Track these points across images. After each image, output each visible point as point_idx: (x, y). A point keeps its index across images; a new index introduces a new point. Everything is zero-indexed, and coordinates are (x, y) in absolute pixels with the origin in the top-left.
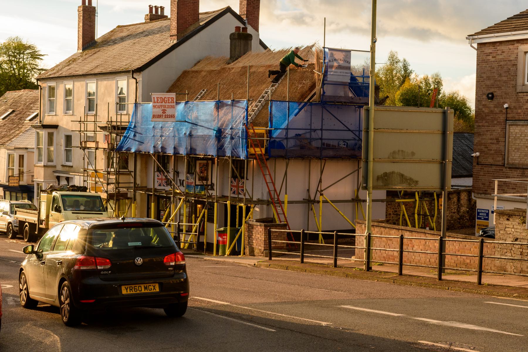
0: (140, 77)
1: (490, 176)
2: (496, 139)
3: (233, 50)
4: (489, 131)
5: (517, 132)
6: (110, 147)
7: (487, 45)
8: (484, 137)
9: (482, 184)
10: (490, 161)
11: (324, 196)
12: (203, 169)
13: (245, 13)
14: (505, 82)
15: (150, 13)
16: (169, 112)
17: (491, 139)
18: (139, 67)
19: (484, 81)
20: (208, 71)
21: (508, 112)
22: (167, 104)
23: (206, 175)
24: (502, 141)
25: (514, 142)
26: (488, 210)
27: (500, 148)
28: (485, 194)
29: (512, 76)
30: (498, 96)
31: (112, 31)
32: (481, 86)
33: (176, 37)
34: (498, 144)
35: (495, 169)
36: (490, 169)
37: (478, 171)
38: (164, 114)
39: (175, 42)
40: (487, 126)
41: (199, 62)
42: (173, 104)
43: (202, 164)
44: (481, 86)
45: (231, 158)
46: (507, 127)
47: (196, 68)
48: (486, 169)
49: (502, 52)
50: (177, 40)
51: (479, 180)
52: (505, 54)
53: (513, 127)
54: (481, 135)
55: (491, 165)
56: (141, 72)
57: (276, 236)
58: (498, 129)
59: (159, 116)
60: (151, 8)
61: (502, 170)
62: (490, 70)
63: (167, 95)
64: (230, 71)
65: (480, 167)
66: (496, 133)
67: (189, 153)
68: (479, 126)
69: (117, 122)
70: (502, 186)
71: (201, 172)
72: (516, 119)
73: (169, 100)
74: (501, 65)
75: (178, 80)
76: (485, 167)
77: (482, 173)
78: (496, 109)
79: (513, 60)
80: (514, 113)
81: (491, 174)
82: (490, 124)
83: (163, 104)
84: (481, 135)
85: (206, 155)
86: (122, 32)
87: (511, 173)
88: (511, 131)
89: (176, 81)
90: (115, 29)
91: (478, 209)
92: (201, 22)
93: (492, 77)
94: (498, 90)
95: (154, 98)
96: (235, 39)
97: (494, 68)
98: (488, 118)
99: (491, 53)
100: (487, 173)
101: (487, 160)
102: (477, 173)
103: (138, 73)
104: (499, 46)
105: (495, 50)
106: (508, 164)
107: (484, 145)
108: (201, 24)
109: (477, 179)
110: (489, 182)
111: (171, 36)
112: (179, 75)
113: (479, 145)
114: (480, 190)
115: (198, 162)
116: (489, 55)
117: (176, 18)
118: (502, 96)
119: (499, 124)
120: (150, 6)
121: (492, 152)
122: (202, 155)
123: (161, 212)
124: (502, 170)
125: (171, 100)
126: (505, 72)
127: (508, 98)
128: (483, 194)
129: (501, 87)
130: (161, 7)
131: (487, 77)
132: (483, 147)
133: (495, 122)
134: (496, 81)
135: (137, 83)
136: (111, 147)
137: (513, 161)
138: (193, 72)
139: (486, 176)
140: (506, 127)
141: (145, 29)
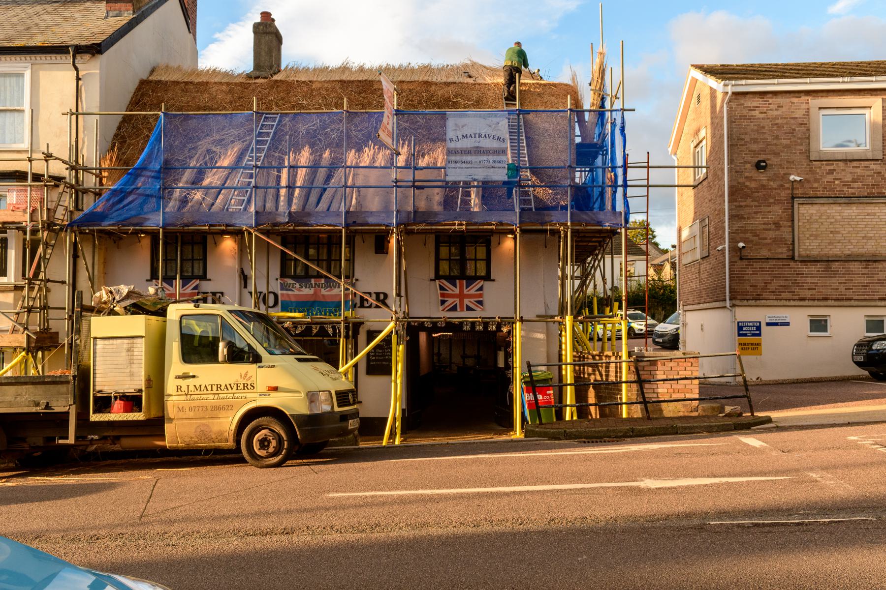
0: (92, 68)
1: (767, 274)
2: (774, 224)
3: (263, 54)
4: (761, 212)
5: (812, 214)
7: (748, 96)
8: (751, 221)
9: (751, 286)
10: (765, 253)
14: (788, 147)
17: (764, 224)
18: (89, 44)
19: (746, 145)
21: (795, 186)
24: (785, 226)
25: (808, 227)
26: (760, 322)
27: (782, 235)
28: (756, 300)
29: (799, 138)
30: (775, 165)
32: (741, 151)
34: (779, 230)
35: (774, 265)
36: (764, 265)
37: (742, 268)
40: (756, 206)
44: (741, 151)
46: (796, 206)
48: (757, 265)
49: (778, 107)
50: (134, 12)
51: (746, 280)
52: (784, 109)
53: (805, 206)
54: (745, 218)
55: (768, 259)
58: (777, 211)
61: (789, 265)
62: (758, 131)
65: (745, 262)
66: (773, 215)
68: (741, 206)
70: (790, 286)
72: (811, 195)
74: (776, 124)
76: (756, 262)
77: (749, 271)
78: (771, 183)
79: (800, 118)
80: (805, 188)
81: (768, 271)
82: (762, 203)
84: (745, 218)
87: (806, 268)
88: (801, 212)
91: (738, 323)
93: (761, 139)
94: (774, 157)
97: (764, 127)
98: (756, 194)
99: (757, 107)
100: (759, 271)
101: (759, 253)
102: (739, 271)
103: (87, 57)
104: (772, 98)
105: (766, 104)
106: (799, 256)
107: (750, 233)
109: (739, 280)
110: (765, 283)
113: (741, 233)
114: (746, 295)
116: (755, 110)
118: (781, 165)
119: (778, 204)
121: (769, 241)
124: (789, 265)
126: (786, 133)
127: (792, 168)
128: (752, 300)
129: (779, 153)
131: (751, 139)
132: (749, 235)
133: (772, 200)
134: (768, 145)
135: (78, 79)
137: (809, 252)
139: (757, 274)
140: (793, 206)
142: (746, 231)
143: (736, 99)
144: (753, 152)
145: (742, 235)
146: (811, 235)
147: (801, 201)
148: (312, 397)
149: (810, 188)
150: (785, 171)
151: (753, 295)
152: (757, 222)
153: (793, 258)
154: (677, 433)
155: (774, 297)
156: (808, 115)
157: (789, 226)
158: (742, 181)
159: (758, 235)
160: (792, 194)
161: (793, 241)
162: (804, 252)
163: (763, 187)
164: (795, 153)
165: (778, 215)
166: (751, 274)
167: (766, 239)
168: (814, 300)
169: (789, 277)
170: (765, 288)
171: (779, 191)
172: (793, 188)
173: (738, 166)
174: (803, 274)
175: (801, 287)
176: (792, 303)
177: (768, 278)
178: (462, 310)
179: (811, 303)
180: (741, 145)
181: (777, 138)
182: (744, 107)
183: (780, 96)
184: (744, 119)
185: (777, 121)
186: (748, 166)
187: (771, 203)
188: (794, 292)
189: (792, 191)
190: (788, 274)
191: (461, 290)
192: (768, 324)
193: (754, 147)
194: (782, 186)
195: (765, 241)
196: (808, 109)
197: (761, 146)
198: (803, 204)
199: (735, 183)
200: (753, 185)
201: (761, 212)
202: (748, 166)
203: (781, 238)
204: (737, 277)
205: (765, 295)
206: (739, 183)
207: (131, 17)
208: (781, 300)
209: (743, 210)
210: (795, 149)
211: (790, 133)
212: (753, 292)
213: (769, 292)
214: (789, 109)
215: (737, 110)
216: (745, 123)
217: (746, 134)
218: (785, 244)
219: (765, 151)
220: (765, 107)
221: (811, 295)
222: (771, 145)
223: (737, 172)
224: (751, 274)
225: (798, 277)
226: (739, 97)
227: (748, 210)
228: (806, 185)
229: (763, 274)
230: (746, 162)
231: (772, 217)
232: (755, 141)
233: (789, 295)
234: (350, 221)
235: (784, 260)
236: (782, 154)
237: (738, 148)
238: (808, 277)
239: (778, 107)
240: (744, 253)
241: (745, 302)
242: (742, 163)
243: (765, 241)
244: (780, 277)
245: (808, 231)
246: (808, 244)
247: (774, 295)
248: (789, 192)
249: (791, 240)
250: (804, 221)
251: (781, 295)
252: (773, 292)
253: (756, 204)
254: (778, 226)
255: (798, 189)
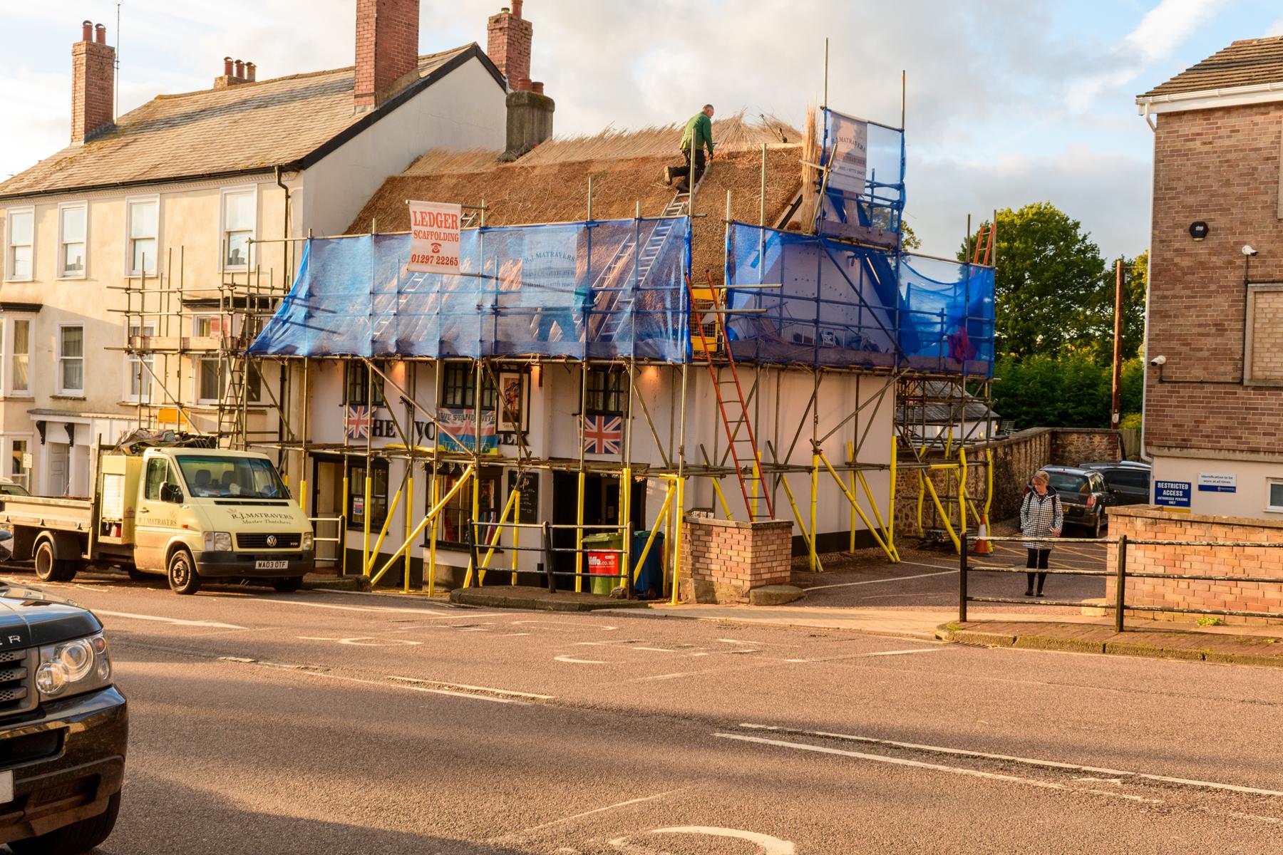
0: (296, 183)
1: (1199, 407)
2: (1215, 325)
3: (515, 131)
4: (1196, 306)
5: (1277, 309)
6: (229, 346)
7: (1185, 117)
8: (1181, 321)
9: (1174, 426)
10: (1198, 373)
11: (823, 455)
12: (512, 393)
13: (504, 62)
14: (1242, 198)
15: (226, 73)
16: (447, 249)
17: (1200, 325)
18: (299, 158)
19: (1179, 198)
20: (460, 176)
21: (1251, 264)
22: (443, 230)
23: (517, 408)
24: (1232, 330)
25: (1269, 330)
26: (1189, 484)
27: (1227, 344)
28: (1182, 448)
29: (1262, 183)
30: (1222, 229)
31: (147, 106)
32: (1169, 208)
33: (373, 98)
34: (1222, 335)
35: (1211, 392)
36: (1198, 392)
37: (1161, 396)
38: (435, 255)
39: (370, 109)
40: (1188, 297)
41: (417, 160)
42: (454, 231)
43: (510, 382)
44: (1169, 208)
45: (633, 362)
46: (1250, 296)
47: (416, 172)
48: (1185, 392)
49: (1232, 131)
50: (376, 105)
51: (1166, 416)
52: (1239, 136)
53: (1266, 296)
54: (1170, 316)
55: (1202, 382)
56: (302, 171)
57: (772, 553)
58: (1221, 305)
59: (425, 260)
60: (229, 65)
61: (1235, 393)
62: (1197, 173)
63: (442, 207)
64: (528, 172)
65: (1168, 387)
66: (1214, 311)
67: (489, 352)
68: (1165, 297)
69: (249, 286)
70: (1236, 428)
71: (509, 401)
72: (1276, 278)
73: (446, 221)
74: (1227, 161)
75: (380, 195)
76: (1184, 387)
77: (1173, 402)
78: (1214, 259)
79: (1266, 148)
80: (1267, 266)
81: (1202, 402)
82: (1197, 292)
83: (435, 229)
84: (1170, 316)
85: (548, 357)
86: (179, 105)
87: (1262, 399)
88: (1259, 305)
89: (374, 198)
90: (152, 102)
91: (1157, 482)
92: (422, 70)
93: (1202, 187)
94: (1221, 215)
95: (415, 212)
96: (519, 106)
97: (1207, 167)
98: (1189, 278)
99: (1198, 134)
100: (1188, 402)
101: (1190, 373)
102: (1158, 401)
103: (293, 174)
104: (1222, 118)
105: (1212, 128)
106: (1251, 379)
107: (1179, 340)
108: (423, 74)
109: (1157, 415)
110: (1196, 422)
111: (356, 97)
112: (380, 187)
113: (1164, 339)
114: (1167, 439)
115: (503, 376)
116: (1194, 140)
117: (373, 54)
118: (1231, 229)
119: (1223, 292)
120: (226, 59)
121: (1205, 354)
122: (534, 357)
123: (356, 499)
124: (1235, 393)
125: (450, 221)
126: (1242, 175)
127: (1248, 233)
128: (1176, 447)
129: (1229, 210)
130: (249, 64)
131: (1187, 188)
132: (1175, 344)
133: (1213, 287)
134: (1212, 196)
135: (288, 197)
136: (232, 345)
137: (1268, 373)
138: (416, 178)
139: (1185, 407)
140: (1246, 296)
141: (244, 97)
142: (1170, 337)
143: (1167, 123)
144: (1189, 209)
145: (1164, 344)
146: (1274, 345)
147: (1258, 287)
148: (209, 535)
149: (1276, 266)
150: (1238, 238)
151: (1177, 440)
152: (1188, 322)
153: (1241, 383)
154: (535, 608)
155: (1210, 445)
156: (1279, 143)
157: (1239, 330)
158: (1169, 257)
159: (1190, 344)
160: (1247, 276)
161: (1243, 354)
162: (1260, 373)
163: (1202, 265)
164: (1255, 208)
165: (1222, 311)
166: (1175, 407)
167: (1201, 350)
168: (1274, 453)
169: (1235, 413)
170: (1195, 430)
171: (1225, 272)
172: (1248, 267)
173: (1164, 232)
174: (1257, 409)
175: (1252, 430)
176: (1238, 456)
177: (1201, 413)
178: (600, 453)
179: (1268, 457)
180: (1170, 198)
181: (1227, 183)
182: (1178, 137)
183: (1234, 114)
184: (1178, 156)
185: (1229, 156)
186: (1180, 232)
187: (1212, 292)
188: (1241, 438)
189: (1247, 272)
190: (1233, 408)
191: (600, 428)
192: (1202, 488)
193: (1191, 200)
194: (1231, 262)
195: (1200, 354)
196: (1280, 132)
197: (1202, 197)
198: (1263, 292)
199: (1159, 260)
200: (1185, 262)
201: (1196, 306)
202: (1180, 232)
203: (1225, 349)
204: (1154, 411)
205: (1195, 440)
206: (1164, 260)
207: (373, 110)
208: (1220, 450)
209: (1169, 303)
210: (1255, 201)
211: (1249, 174)
212: (1178, 435)
213: (1202, 436)
214: (1249, 135)
215: (1166, 142)
216: (1178, 161)
217: (1179, 179)
218: (1230, 359)
219: (1207, 206)
220: (1212, 134)
221: (1268, 444)
222: (1218, 195)
223: (1162, 241)
224: (1175, 407)
225: (1249, 414)
226: (1170, 120)
227: (1175, 303)
228: (1270, 261)
229: (1194, 407)
230: (1177, 226)
231: (1212, 315)
232: (1192, 190)
233: (1232, 443)
234: (445, 352)
235: (1228, 386)
236: (1234, 211)
237: (1166, 204)
238: (1264, 414)
239: (1232, 131)
240: (1166, 372)
241: (1166, 452)
242: (1170, 227)
243: (1200, 354)
244: (1220, 413)
245: (1269, 337)
246: (1268, 360)
247: (1209, 442)
248: (1242, 273)
249: (1241, 352)
250: (1264, 321)
251: (1219, 442)
252: (1207, 436)
253: (1188, 292)
254: (1220, 328)
255: (1257, 267)
